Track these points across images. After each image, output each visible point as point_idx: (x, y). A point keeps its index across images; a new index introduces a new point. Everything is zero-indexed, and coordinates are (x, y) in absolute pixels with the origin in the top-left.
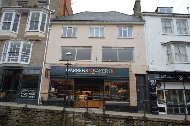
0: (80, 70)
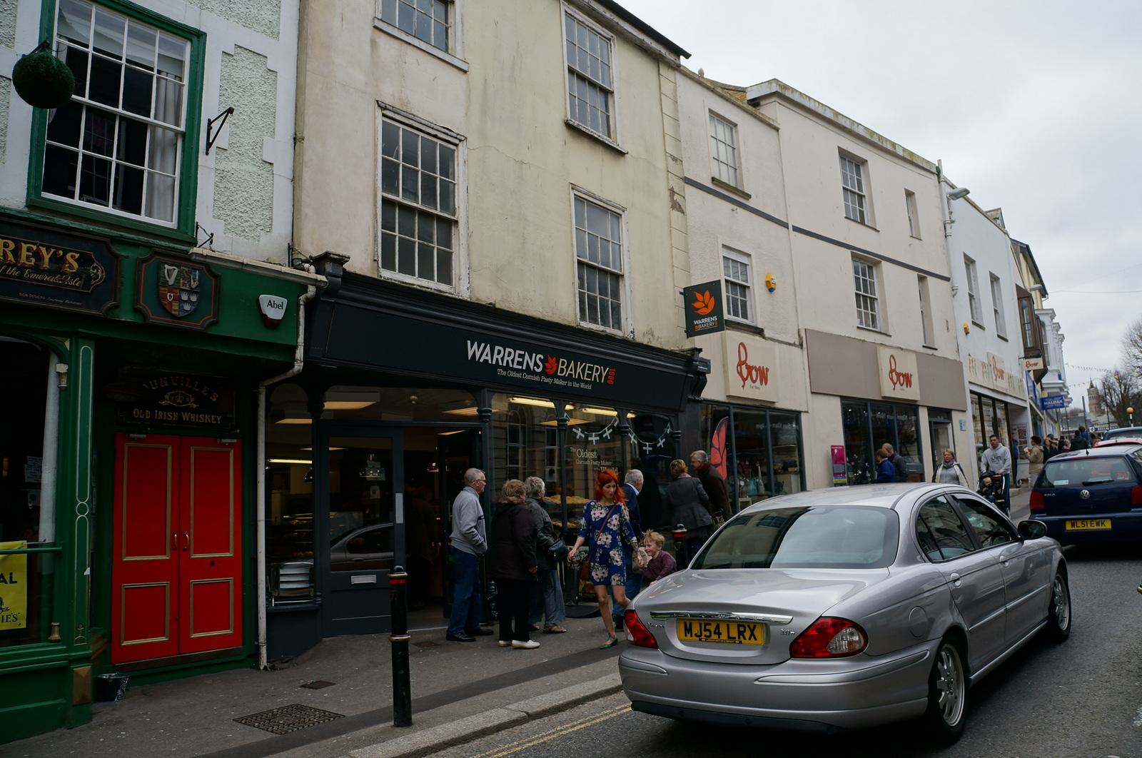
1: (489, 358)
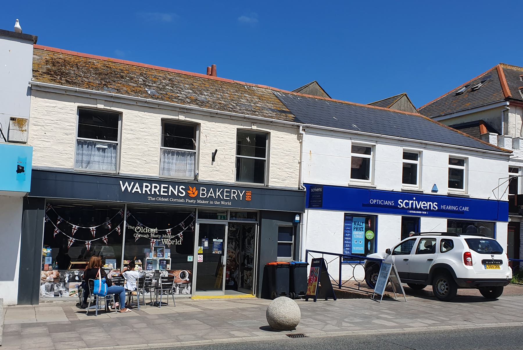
0: (164, 187)
1: (139, 190)
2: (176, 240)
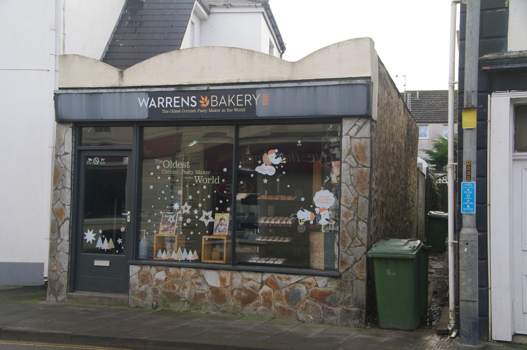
1: (154, 105)
2: (213, 177)
